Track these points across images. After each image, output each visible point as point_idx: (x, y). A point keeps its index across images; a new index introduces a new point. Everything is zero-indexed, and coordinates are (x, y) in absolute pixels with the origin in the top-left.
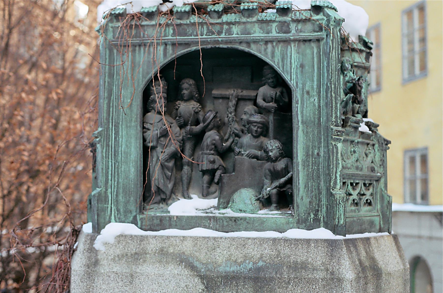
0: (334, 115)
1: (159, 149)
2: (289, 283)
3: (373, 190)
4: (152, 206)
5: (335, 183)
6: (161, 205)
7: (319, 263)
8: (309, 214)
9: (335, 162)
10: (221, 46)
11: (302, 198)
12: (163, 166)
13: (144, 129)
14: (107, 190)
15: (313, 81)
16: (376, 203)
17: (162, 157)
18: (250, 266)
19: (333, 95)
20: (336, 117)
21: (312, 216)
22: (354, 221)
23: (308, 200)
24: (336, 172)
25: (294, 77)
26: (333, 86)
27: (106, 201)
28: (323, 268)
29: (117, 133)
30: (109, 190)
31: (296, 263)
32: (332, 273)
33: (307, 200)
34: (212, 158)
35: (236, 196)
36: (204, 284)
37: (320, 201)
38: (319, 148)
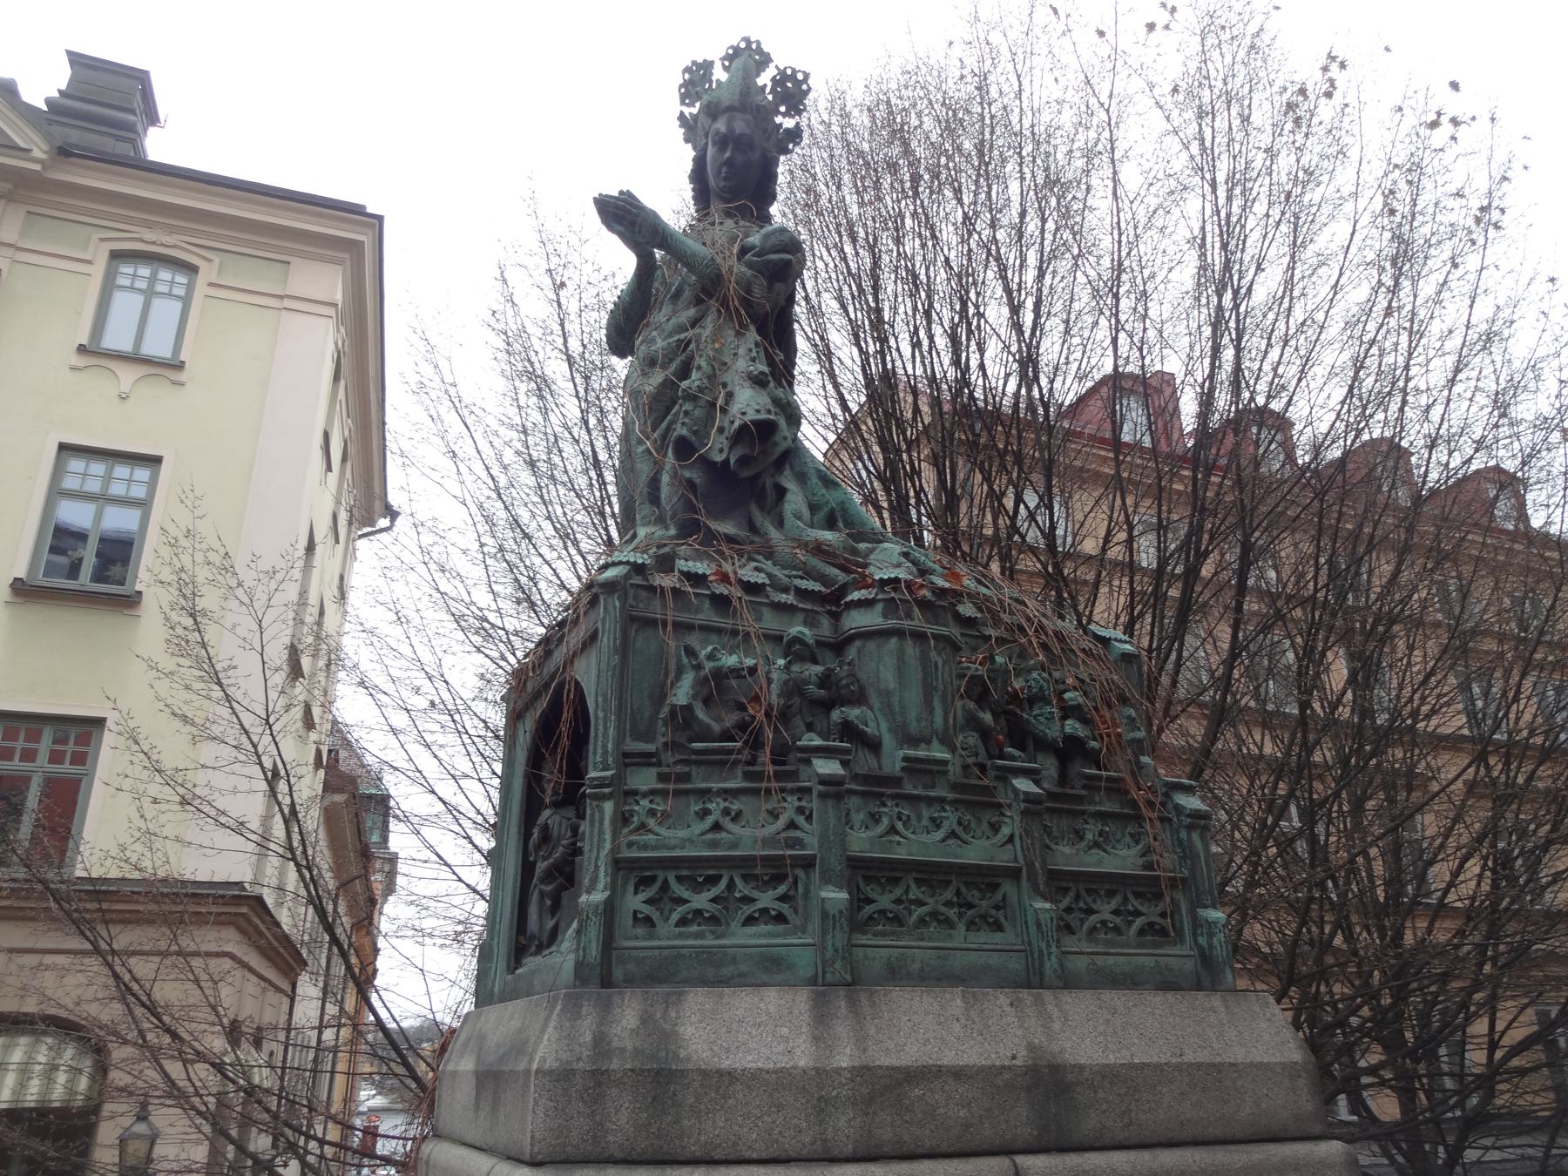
0: (600, 751)
5: (594, 880)
19: (601, 714)
20: (605, 753)
22: (680, 956)
24: (597, 859)
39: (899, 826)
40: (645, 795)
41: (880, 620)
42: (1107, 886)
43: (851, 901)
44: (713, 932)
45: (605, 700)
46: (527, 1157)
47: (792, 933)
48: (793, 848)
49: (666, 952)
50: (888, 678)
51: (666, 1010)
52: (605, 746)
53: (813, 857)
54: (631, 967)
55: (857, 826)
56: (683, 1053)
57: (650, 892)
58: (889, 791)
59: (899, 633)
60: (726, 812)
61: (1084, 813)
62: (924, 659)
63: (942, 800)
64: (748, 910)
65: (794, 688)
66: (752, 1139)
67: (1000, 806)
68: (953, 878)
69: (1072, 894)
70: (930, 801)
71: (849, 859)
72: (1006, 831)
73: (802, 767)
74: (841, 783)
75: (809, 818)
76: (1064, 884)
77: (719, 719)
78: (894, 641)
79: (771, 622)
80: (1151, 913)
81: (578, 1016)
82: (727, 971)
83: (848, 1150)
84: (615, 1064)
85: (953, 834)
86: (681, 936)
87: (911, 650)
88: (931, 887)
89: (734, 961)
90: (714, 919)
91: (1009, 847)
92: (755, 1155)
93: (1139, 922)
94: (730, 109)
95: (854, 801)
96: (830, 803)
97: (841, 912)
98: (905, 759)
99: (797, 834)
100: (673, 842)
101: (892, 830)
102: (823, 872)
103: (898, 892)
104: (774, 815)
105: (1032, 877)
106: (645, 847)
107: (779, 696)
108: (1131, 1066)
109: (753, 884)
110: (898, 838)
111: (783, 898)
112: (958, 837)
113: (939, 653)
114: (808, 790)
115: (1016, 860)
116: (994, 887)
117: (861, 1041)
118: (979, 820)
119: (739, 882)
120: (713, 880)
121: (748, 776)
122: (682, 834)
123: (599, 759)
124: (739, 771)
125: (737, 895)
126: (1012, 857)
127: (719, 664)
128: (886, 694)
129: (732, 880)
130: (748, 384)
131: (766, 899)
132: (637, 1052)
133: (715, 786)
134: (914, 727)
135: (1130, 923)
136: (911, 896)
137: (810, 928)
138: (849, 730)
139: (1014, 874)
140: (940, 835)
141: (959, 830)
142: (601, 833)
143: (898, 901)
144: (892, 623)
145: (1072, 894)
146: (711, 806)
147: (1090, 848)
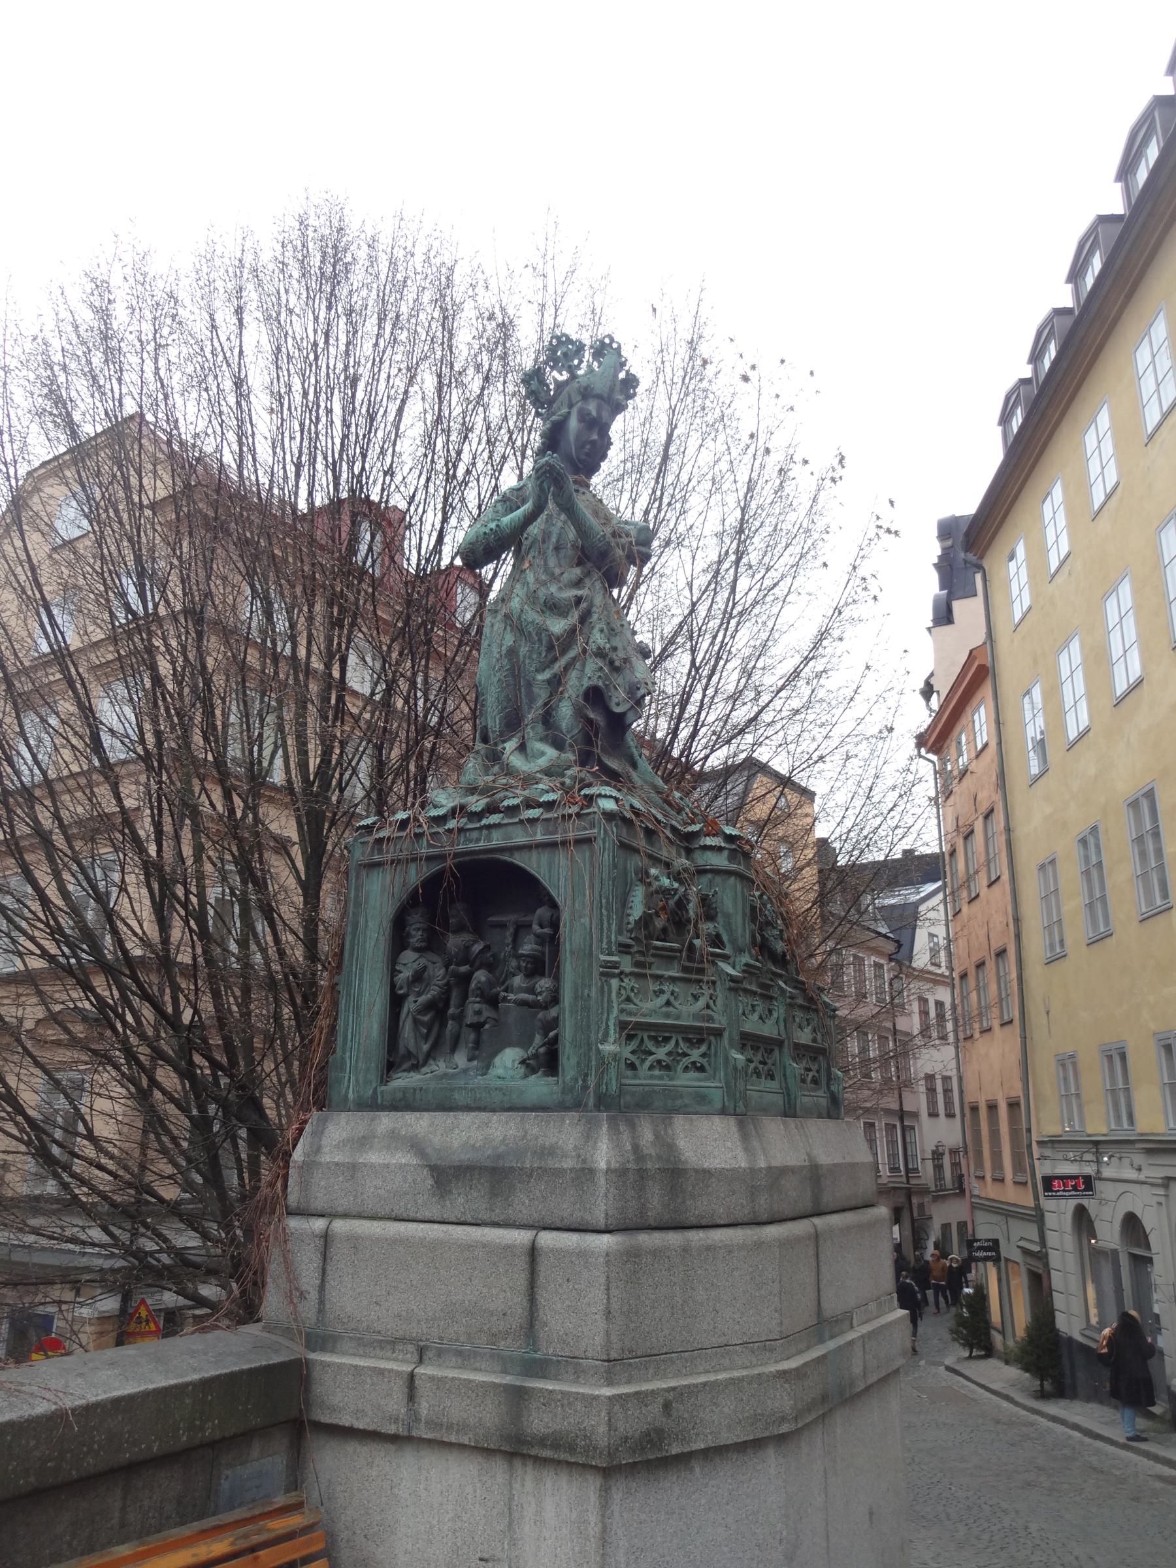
1: (411, 998)
2: (531, 1176)
3: (709, 1048)
4: (400, 1075)
6: (412, 1074)
7: (571, 1146)
8: (576, 1080)
9: (605, 1005)
10: (481, 857)
11: (568, 1059)
12: (416, 1022)
13: (394, 972)
14: (344, 1053)
15: (584, 895)
16: (715, 1070)
17: (413, 1007)
18: (489, 1152)
19: (605, 912)
20: (609, 942)
21: (580, 1082)
22: (654, 1091)
23: (576, 1059)
24: (608, 1020)
25: (562, 891)
26: (604, 901)
27: (343, 1069)
28: (573, 1154)
29: (361, 980)
30: (348, 1054)
31: (543, 1147)
32: (584, 1161)
33: (574, 1061)
34: (477, 1006)
35: (497, 1060)
36: (433, 1177)
37: (590, 1060)
38: (590, 986)
41: (726, 863)
46: (602, 1226)
48: (708, 1021)
49: (647, 1088)
51: (666, 1130)
52: (609, 937)
54: (628, 1098)
56: (683, 1159)
57: (634, 1045)
63: (755, 993)
72: (775, 1015)
82: (678, 1102)
86: (652, 1077)
89: (681, 1096)
92: (722, 1222)
94: (599, 397)
99: (710, 1012)
104: (696, 998)
106: (630, 1014)
108: (834, 1164)
111: (703, 1055)
120: (667, 1040)
121: (686, 969)
123: (605, 946)
124: (676, 963)
128: (727, 916)
131: (695, 1054)
132: (659, 1157)
139: (780, 1044)
142: (610, 1001)
144: (733, 867)
146: (665, 988)
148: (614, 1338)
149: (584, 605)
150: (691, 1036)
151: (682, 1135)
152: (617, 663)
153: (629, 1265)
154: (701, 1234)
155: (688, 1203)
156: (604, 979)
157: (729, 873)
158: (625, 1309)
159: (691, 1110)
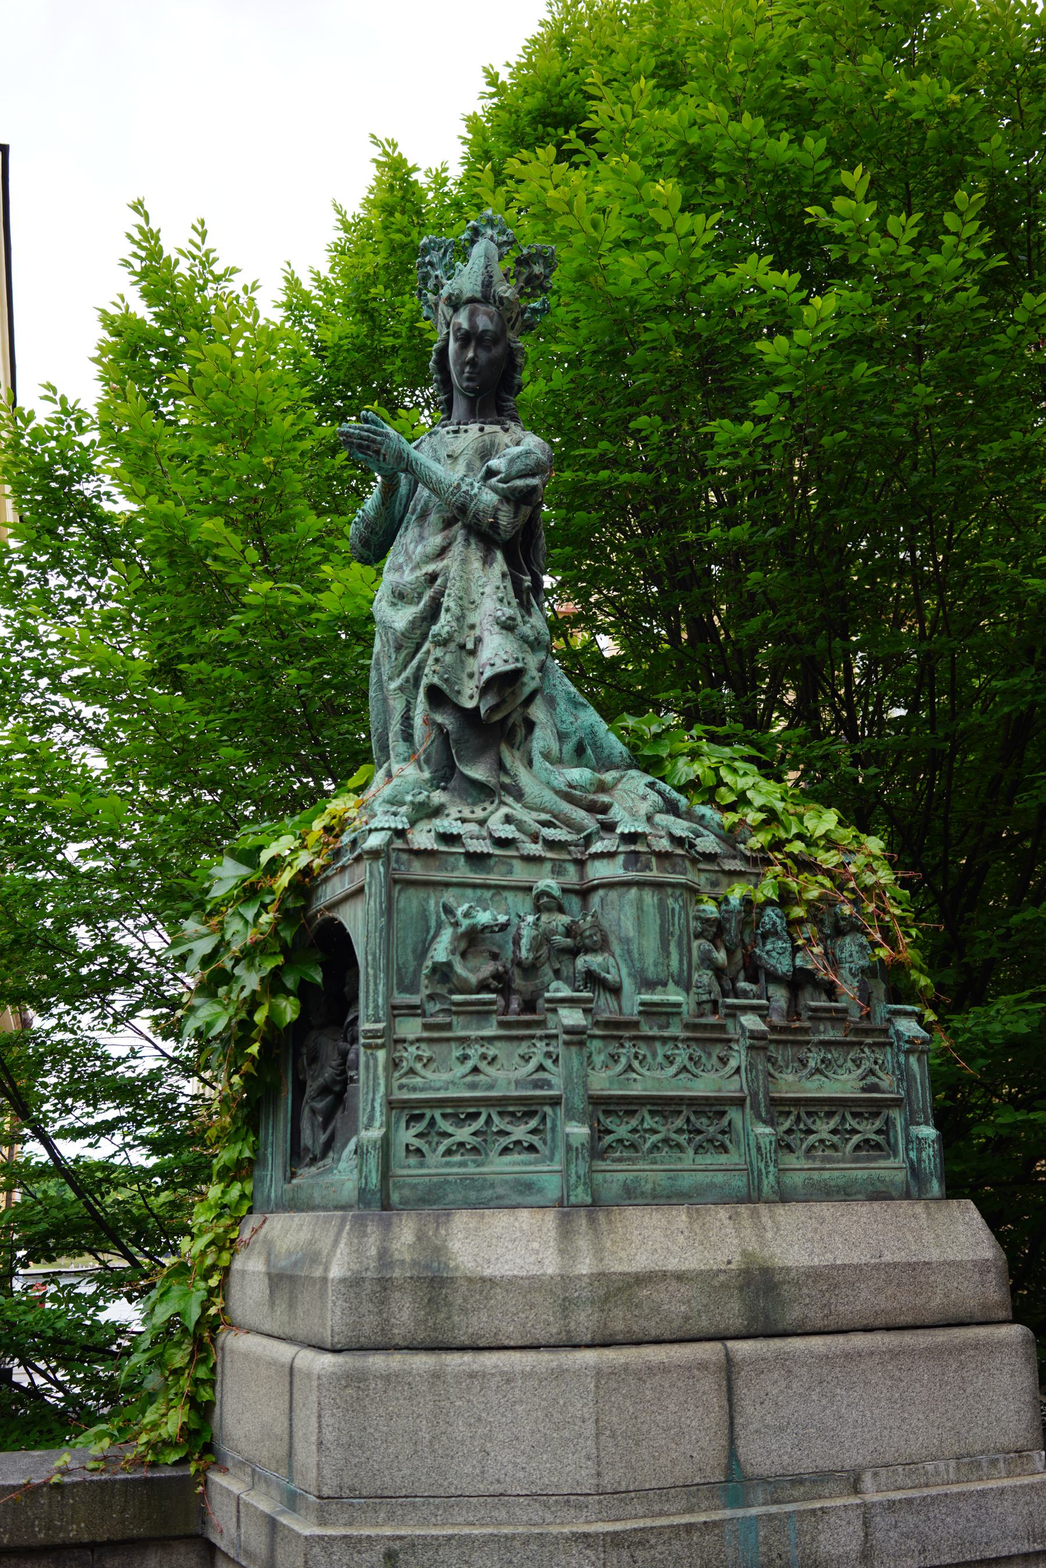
0: (371, 1005)
5: (371, 1119)
19: (371, 971)
20: (376, 1007)
22: (447, 1182)
24: (373, 1100)
26: (370, 958)
30: (270, 1150)
39: (636, 1064)
40: (412, 1043)
41: (621, 871)
42: (826, 1109)
43: (592, 1136)
44: (474, 1161)
45: (374, 959)
46: (329, 1346)
47: (542, 1162)
48: (542, 1088)
49: (435, 1179)
50: (629, 927)
52: (375, 1001)
53: (560, 1097)
54: (407, 1192)
55: (598, 1066)
56: (452, 1264)
57: (420, 1127)
58: (627, 1034)
59: (641, 884)
60: (484, 1057)
61: (808, 1042)
62: (662, 906)
63: (675, 1039)
64: (504, 1141)
65: (543, 940)
66: (511, 1333)
67: (730, 1040)
68: (684, 1108)
69: (792, 1117)
70: (664, 1040)
71: (590, 1097)
72: (733, 1063)
73: (549, 1016)
74: (583, 1033)
75: (556, 1061)
76: (787, 1109)
77: (474, 970)
78: (634, 891)
79: (521, 873)
80: (868, 1129)
81: (365, 1234)
82: (488, 1193)
83: (587, 1338)
84: (397, 1273)
85: (684, 1069)
86: (448, 1164)
87: (649, 898)
88: (665, 1117)
89: (492, 1186)
90: (475, 1150)
91: (736, 1077)
92: (512, 1343)
93: (856, 1139)
94: (472, 300)
95: (596, 1044)
96: (574, 1049)
97: (583, 1145)
98: (642, 1004)
100: (438, 1084)
101: (630, 1068)
102: (567, 1111)
103: (634, 1123)
104: (525, 1058)
105: (755, 1106)
106: (414, 1089)
107: (529, 951)
108: (833, 1267)
109: (508, 1119)
110: (635, 1076)
111: (533, 1132)
112: (688, 1071)
113: (676, 900)
114: (555, 1037)
115: (741, 1090)
116: (723, 1113)
117: (599, 1252)
118: (709, 1055)
119: (496, 1118)
121: (502, 1025)
122: (445, 1076)
123: (371, 1012)
124: (494, 1019)
125: (495, 1129)
126: (738, 1087)
127: (474, 921)
128: (626, 941)
129: (489, 1116)
130: (496, 628)
131: (520, 1132)
132: (415, 1263)
133: (473, 1033)
134: (651, 973)
135: (847, 1140)
136: (646, 1126)
137: (557, 1157)
138: (592, 979)
139: (739, 1102)
140: (673, 1070)
141: (690, 1066)
142: (376, 1077)
143: (634, 1131)
144: (632, 875)
145: (792, 1117)
146: (470, 1052)
147: (812, 1075)
148: (327, 1472)
149: (439, 581)
150: (511, 1109)
151: (460, 1236)
152: (470, 646)
153: (349, 1391)
154: (467, 1357)
155: (456, 1319)
156: (369, 1052)
157: (627, 884)
158: (345, 1440)
159: (507, 1202)
